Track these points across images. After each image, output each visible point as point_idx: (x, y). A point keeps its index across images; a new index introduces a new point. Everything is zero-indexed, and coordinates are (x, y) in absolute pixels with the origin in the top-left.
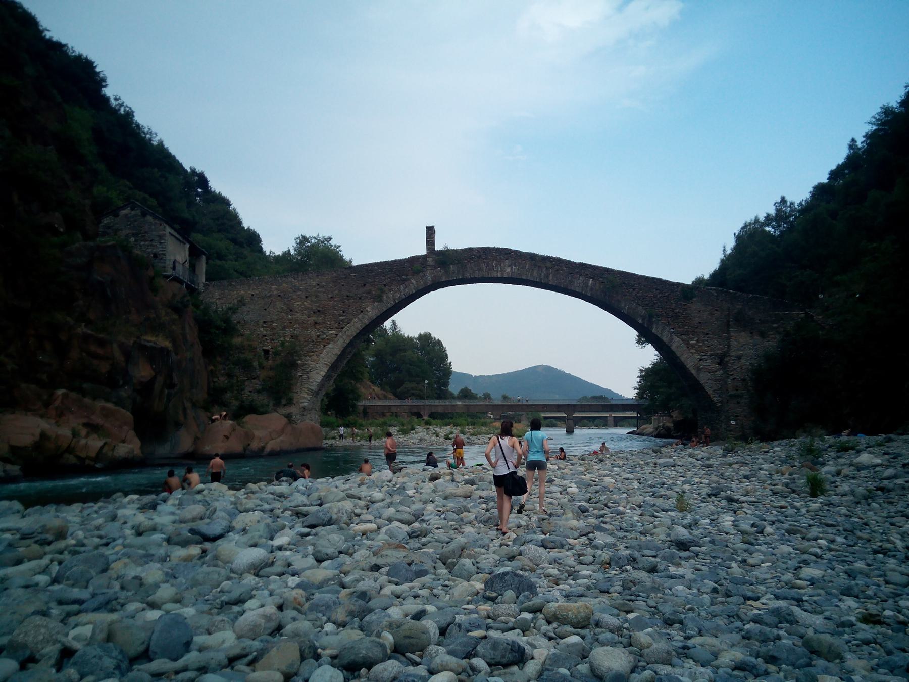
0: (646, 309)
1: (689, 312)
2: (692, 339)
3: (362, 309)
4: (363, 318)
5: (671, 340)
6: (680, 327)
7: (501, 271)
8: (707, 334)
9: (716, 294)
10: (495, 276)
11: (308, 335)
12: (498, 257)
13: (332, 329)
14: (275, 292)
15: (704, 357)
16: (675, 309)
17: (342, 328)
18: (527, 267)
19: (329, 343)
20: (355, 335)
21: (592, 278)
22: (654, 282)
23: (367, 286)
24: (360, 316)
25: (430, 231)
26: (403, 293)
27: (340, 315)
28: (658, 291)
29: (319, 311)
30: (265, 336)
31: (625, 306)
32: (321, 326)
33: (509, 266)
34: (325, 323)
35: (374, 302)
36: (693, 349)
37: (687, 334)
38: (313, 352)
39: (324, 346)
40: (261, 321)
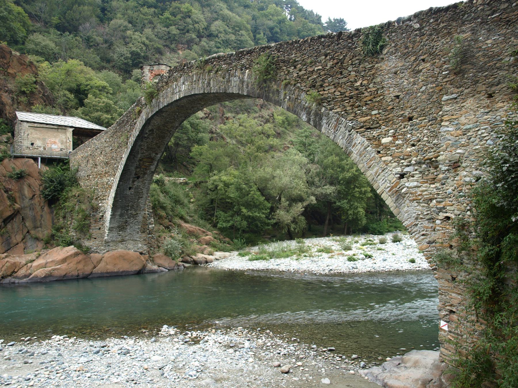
1: (379, 80)
2: (386, 135)
5: (350, 141)
6: (363, 114)
9: (417, 26)
10: (175, 99)
15: (407, 169)
16: (356, 81)
27: (115, 164)
33: (183, 83)
36: (387, 155)
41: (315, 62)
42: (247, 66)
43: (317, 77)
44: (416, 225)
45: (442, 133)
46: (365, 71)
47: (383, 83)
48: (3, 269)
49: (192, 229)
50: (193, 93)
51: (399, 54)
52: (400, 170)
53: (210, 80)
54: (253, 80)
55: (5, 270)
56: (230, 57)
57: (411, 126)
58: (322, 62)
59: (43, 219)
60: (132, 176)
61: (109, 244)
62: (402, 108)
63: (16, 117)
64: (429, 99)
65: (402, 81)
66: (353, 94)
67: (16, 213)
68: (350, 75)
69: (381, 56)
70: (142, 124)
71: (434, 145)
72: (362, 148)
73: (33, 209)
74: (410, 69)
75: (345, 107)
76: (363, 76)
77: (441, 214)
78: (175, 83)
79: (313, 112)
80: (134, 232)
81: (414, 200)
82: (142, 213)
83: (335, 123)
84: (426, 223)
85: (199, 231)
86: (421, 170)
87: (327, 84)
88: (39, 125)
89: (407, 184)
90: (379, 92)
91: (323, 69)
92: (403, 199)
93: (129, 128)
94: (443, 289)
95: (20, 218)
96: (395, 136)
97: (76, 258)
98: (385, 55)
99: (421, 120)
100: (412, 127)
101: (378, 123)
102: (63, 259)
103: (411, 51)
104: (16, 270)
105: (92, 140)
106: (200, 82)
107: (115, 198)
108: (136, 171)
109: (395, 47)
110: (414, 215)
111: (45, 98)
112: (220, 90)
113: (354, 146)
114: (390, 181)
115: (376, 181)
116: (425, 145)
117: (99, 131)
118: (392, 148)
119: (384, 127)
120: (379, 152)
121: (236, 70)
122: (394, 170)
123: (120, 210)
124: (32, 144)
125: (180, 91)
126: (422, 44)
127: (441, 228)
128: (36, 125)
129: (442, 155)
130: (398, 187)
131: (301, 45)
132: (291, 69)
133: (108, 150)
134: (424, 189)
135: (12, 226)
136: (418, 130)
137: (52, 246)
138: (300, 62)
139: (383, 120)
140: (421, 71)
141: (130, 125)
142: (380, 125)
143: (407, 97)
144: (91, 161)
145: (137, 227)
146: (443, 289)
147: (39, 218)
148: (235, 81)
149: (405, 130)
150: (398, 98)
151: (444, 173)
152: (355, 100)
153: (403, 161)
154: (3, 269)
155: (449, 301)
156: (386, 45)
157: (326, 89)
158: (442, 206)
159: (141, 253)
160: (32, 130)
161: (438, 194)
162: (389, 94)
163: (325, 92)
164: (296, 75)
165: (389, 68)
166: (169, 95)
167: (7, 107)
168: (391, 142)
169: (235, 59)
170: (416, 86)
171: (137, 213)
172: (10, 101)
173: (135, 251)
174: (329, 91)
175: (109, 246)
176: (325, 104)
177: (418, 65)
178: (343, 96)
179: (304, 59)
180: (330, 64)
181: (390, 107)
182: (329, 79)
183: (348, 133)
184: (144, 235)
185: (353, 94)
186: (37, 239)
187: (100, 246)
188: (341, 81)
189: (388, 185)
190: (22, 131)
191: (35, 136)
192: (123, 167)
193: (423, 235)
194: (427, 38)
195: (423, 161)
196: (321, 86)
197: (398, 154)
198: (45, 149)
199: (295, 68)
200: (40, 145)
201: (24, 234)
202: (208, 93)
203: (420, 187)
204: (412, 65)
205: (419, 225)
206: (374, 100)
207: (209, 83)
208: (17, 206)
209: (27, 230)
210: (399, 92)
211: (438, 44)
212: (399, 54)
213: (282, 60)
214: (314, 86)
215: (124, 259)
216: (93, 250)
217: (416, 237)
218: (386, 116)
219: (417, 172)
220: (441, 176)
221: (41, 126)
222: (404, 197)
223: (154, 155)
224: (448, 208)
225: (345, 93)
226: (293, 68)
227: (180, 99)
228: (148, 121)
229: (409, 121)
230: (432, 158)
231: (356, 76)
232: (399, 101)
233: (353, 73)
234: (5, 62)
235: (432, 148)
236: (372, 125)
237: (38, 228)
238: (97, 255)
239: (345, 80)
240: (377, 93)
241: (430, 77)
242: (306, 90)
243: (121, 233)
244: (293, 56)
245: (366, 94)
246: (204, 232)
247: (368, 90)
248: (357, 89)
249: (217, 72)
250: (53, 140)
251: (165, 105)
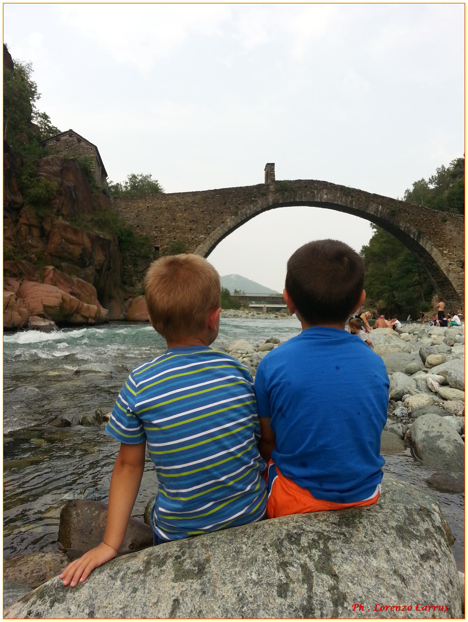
0: (416, 228)
1: (444, 231)
2: (445, 250)
3: (223, 221)
4: (224, 227)
5: (432, 249)
6: (438, 241)
7: (320, 197)
8: (455, 247)
10: (316, 200)
11: (186, 238)
12: (319, 188)
13: (202, 234)
14: (164, 206)
15: (452, 262)
17: (209, 234)
18: (338, 196)
19: (200, 244)
20: (218, 239)
21: (381, 205)
22: (422, 210)
23: (227, 204)
24: (222, 226)
25: (270, 168)
26: (252, 210)
27: (208, 224)
28: (425, 216)
29: (193, 221)
30: (156, 237)
31: (403, 225)
32: (194, 232)
33: (326, 194)
34: (197, 230)
35: (232, 216)
38: (189, 250)
39: (197, 246)
40: (154, 226)
84: (457, 280)
168: (447, 253)
251: (304, 200)
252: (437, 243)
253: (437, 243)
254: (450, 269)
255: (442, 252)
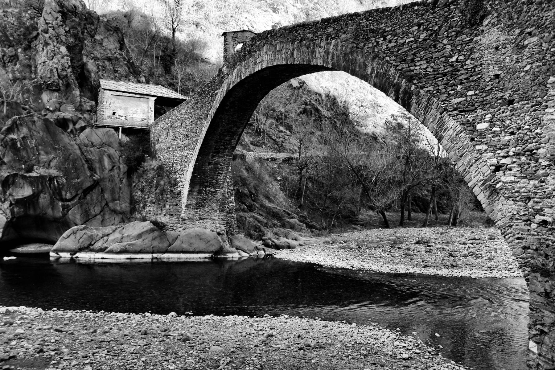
2: (482, 120)
10: (257, 70)
15: (503, 161)
27: (195, 137)
36: (482, 143)
37: (469, 107)
41: (407, 33)
42: (333, 36)
43: (408, 50)
44: (511, 226)
45: (545, 122)
46: (462, 44)
47: (482, 60)
48: (81, 240)
49: (276, 210)
50: (275, 64)
51: (502, 25)
52: (496, 162)
53: (293, 50)
54: (339, 52)
55: (83, 242)
56: (316, 25)
57: (511, 111)
58: (415, 33)
59: (121, 191)
60: (211, 151)
61: (185, 222)
62: (502, 89)
63: (99, 86)
64: (534, 80)
65: (504, 57)
66: (447, 70)
67: (96, 184)
68: (445, 48)
69: (481, 28)
70: (222, 96)
71: (537, 134)
72: (455, 134)
73: (112, 181)
74: (513, 43)
75: (438, 86)
76: (459, 51)
77: (538, 216)
78: (258, 52)
79: (402, 89)
80: (213, 211)
81: (509, 197)
82: (222, 190)
83: (426, 103)
84: (522, 225)
85: (283, 213)
86: (518, 162)
87: (419, 59)
88: (121, 94)
89: (503, 179)
90: (477, 70)
91: (416, 41)
92: (498, 196)
93: (210, 99)
94: (534, 305)
95: (99, 190)
96: (492, 122)
97: (151, 234)
98: (486, 26)
99: (523, 105)
100: (512, 112)
101: (474, 105)
102: (139, 234)
103: (515, 23)
104: (92, 243)
105: (173, 110)
106: (283, 52)
107: (193, 173)
108: (216, 146)
109: (497, 17)
110: (509, 214)
111: (129, 66)
112: (304, 61)
113: (445, 130)
114: (484, 174)
115: (468, 173)
116: (526, 134)
117: (180, 101)
118: (487, 136)
119: (480, 110)
120: (472, 139)
121: (321, 40)
122: (488, 161)
123: (198, 187)
124: (114, 113)
125: (262, 61)
126: (530, 14)
127: (536, 233)
128: (118, 93)
129: (543, 147)
130: (492, 181)
131: (392, 14)
132: (381, 40)
133: (188, 122)
134: (522, 185)
135: (91, 198)
136: (519, 116)
137: (129, 221)
138: (390, 33)
139: (480, 102)
140: (526, 46)
141: (211, 96)
142: (476, 109)
143: (509, 77)
144: (171, 133)
145: (215, 205)
146: (534, 305)
147: (117, 190)
148: (320, 52)
149: (504, 115)
150: (498, 78)
151: (543, 169)
152: (449, 78)
153: (499, 151)
154: (81, 240)
155: (540, 319)
156: (487, 15)
157: (418, 64)
158: (539, 208)
159: (219, 234)
160: (114, 99)
161: (535, 193)
162: (489, 72)
163: (417, 68)
164: (386, 47)
165: (489, 42)
166: (251, 64)
167: (93, 75)
168: (487, 129)
169: (321, 28)
170: (520, 64)
171: (216, 191)
172: (95, 69)
173: (213, 231)
174: (421, 66)
175: (185, 223)
176: (415, 82)
177: (524, 39)
178: (436, 73)
179: (394, 30)
180: (422, 36)
181: (488, 88)
182: (421, 53)
183: (439, 116)
184: (222, 214)
185: (447, 70)
186: (114, 211)
187: (176, 223)
188: (434, 56)
189: (482, 178)
190: (105, 100)
191: (118, 105)
192: (202, 140)
193: (518, 238)
194: (535, 7)
195: (522, 152)
196: (413, 60)
197: (494, 144)
198: (126, 119)
199: (385, 39)
200: (121, 115)
201: (103, 205)
202: (291, 64)
203: (517, 182)
204: (516, 39)
205: (513, 227)
206: (471, 79)
207: (292, 54)
208: (96, 177)
209: (105, 202)
210: (499, 70)
211: (548, 14)
212: (502, 25)
213: (370, 30)
214: (405, 60)
215: (201, 239)
216: (169, 226)
217: (510, 240)
218: (483, 98)
219: (515, 165)
220: (540, 172)
221: (124, 94)
222: (499, 193)
223: (235, 128)
224: (546, 210)
225: (438, 69)
226: (382, 39)
227: (262, 70)
228: (230, 93)
229: (509, 105)
230: (533, 150)
231: (452, 50)
232: (499, 82)
233: (448, 47)
234: (93, 28)
235: (534, 138)
236: (467, 107)
237: (116, 200)
238: (172, 232)
239: (439, 54)
240: (475, 71)
241: (536, 54)
242: (396, 64)
243: (198, 210)
244: (383, 25)
245: (462, 72)
246: (289, 214)
247: (465, 67)
248: (452, 66)
249: (301, 41)
250: (135, 109)
252: (457, 100)
253: (457, 100)
254: (498, 186)
255: (470, 126)
